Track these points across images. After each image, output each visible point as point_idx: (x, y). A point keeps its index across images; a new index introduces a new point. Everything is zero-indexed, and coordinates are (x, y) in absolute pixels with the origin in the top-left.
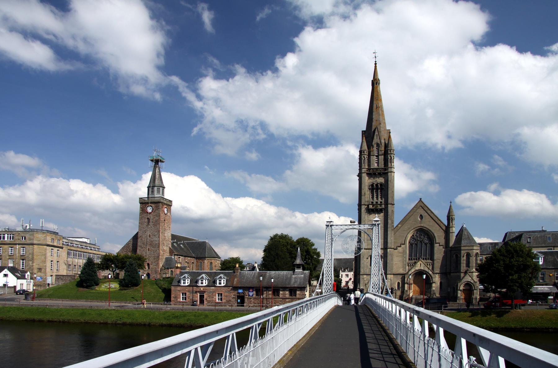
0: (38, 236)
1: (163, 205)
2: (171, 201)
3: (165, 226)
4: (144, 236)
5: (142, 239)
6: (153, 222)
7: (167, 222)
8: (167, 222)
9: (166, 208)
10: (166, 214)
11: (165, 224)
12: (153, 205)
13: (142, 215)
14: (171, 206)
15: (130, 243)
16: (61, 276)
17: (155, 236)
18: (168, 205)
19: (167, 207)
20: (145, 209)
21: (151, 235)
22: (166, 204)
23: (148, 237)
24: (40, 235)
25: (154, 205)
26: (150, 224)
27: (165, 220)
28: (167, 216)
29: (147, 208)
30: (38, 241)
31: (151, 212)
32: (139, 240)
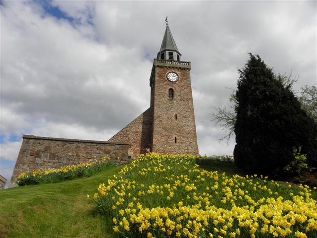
4: (165, 117)
5: (161, 121)
6: (180, 96)
12: (178, 73)
13: (161, 84)
15: (128, 129)
16: (53, 144)
17: (185, 117)
20: (166, 76)
21: (177, 115)
23: (174, 118)
25: (180, 72)
26: (175, 97)
29: (168, 74)
31: (176, 81)
32: (156, 122)
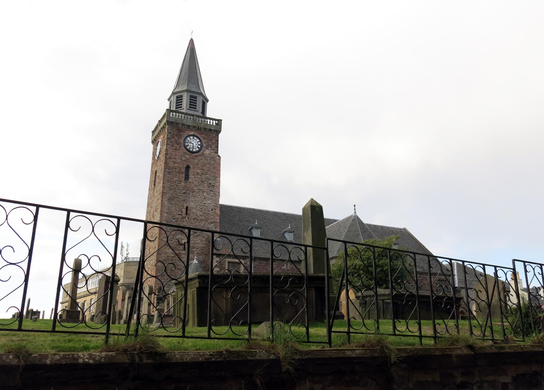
0: (129, 270)
1: (180, 130)
2: (220, 121)
3: (190, 180)
7: (200, 171)
8: (200, 171)
9: (193, 136)
10: (193, 152)
11: (187, 178)
14: (220, 132)
18: (205, 129)
19: (199, 136)
22: (194, 127)
24: (132, 267)
27: (188, 168)
28: (200, 158)
30: (129, 278)
